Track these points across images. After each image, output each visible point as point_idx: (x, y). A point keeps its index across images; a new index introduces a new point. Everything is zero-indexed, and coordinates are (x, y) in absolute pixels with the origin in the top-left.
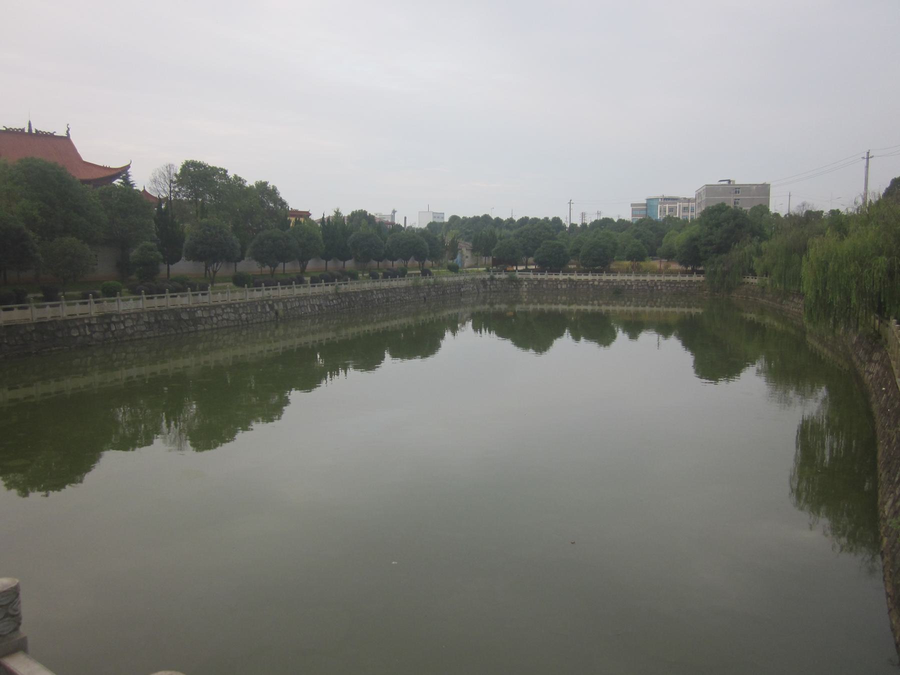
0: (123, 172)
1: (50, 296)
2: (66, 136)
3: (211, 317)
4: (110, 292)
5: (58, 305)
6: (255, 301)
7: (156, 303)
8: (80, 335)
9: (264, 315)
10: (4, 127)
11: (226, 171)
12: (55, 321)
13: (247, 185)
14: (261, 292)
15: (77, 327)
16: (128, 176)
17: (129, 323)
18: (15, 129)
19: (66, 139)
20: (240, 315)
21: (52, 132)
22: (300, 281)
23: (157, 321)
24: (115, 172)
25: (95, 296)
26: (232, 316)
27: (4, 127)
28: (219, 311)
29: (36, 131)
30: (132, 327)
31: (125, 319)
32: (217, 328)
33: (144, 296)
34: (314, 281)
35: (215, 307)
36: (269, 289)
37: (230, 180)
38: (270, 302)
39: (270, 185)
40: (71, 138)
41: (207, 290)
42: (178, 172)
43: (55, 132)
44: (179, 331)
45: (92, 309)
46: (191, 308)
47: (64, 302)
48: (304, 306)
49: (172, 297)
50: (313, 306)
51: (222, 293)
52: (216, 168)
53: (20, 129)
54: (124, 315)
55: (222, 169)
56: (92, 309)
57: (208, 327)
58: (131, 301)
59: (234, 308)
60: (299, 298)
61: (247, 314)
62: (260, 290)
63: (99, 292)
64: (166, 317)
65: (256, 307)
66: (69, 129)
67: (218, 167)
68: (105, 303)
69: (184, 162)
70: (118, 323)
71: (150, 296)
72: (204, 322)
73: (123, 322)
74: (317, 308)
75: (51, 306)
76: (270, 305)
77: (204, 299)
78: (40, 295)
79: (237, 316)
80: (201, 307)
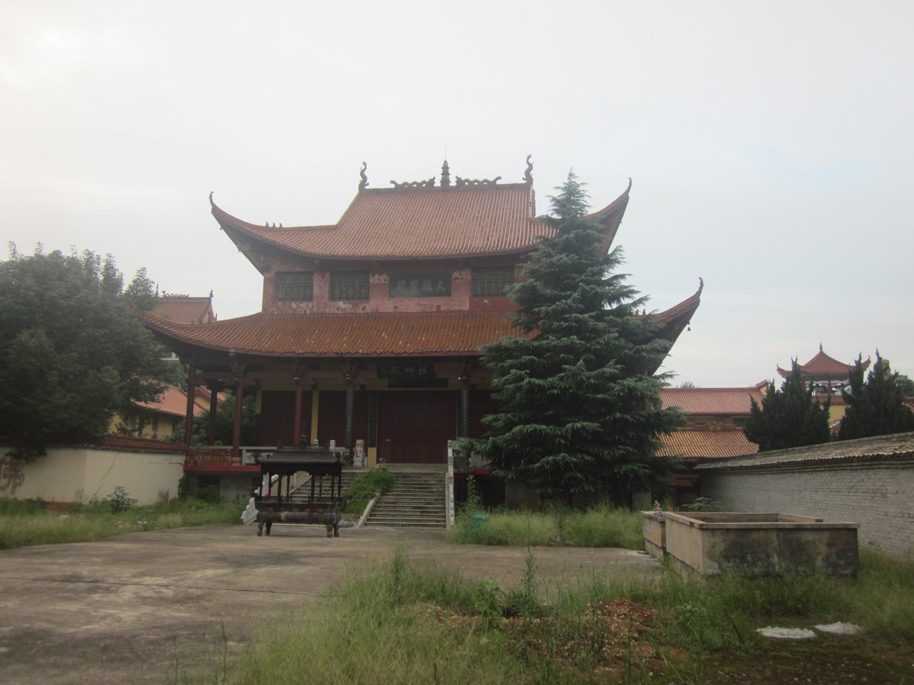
2: (524, 182)
10: (392, 182)
18: (415, 183)
21: (491, 179)
27: (392, 182)
29: (459, 181)
40: (535, 186)
43: (499, 178)
53: (424, 182)
66: (531, 167)
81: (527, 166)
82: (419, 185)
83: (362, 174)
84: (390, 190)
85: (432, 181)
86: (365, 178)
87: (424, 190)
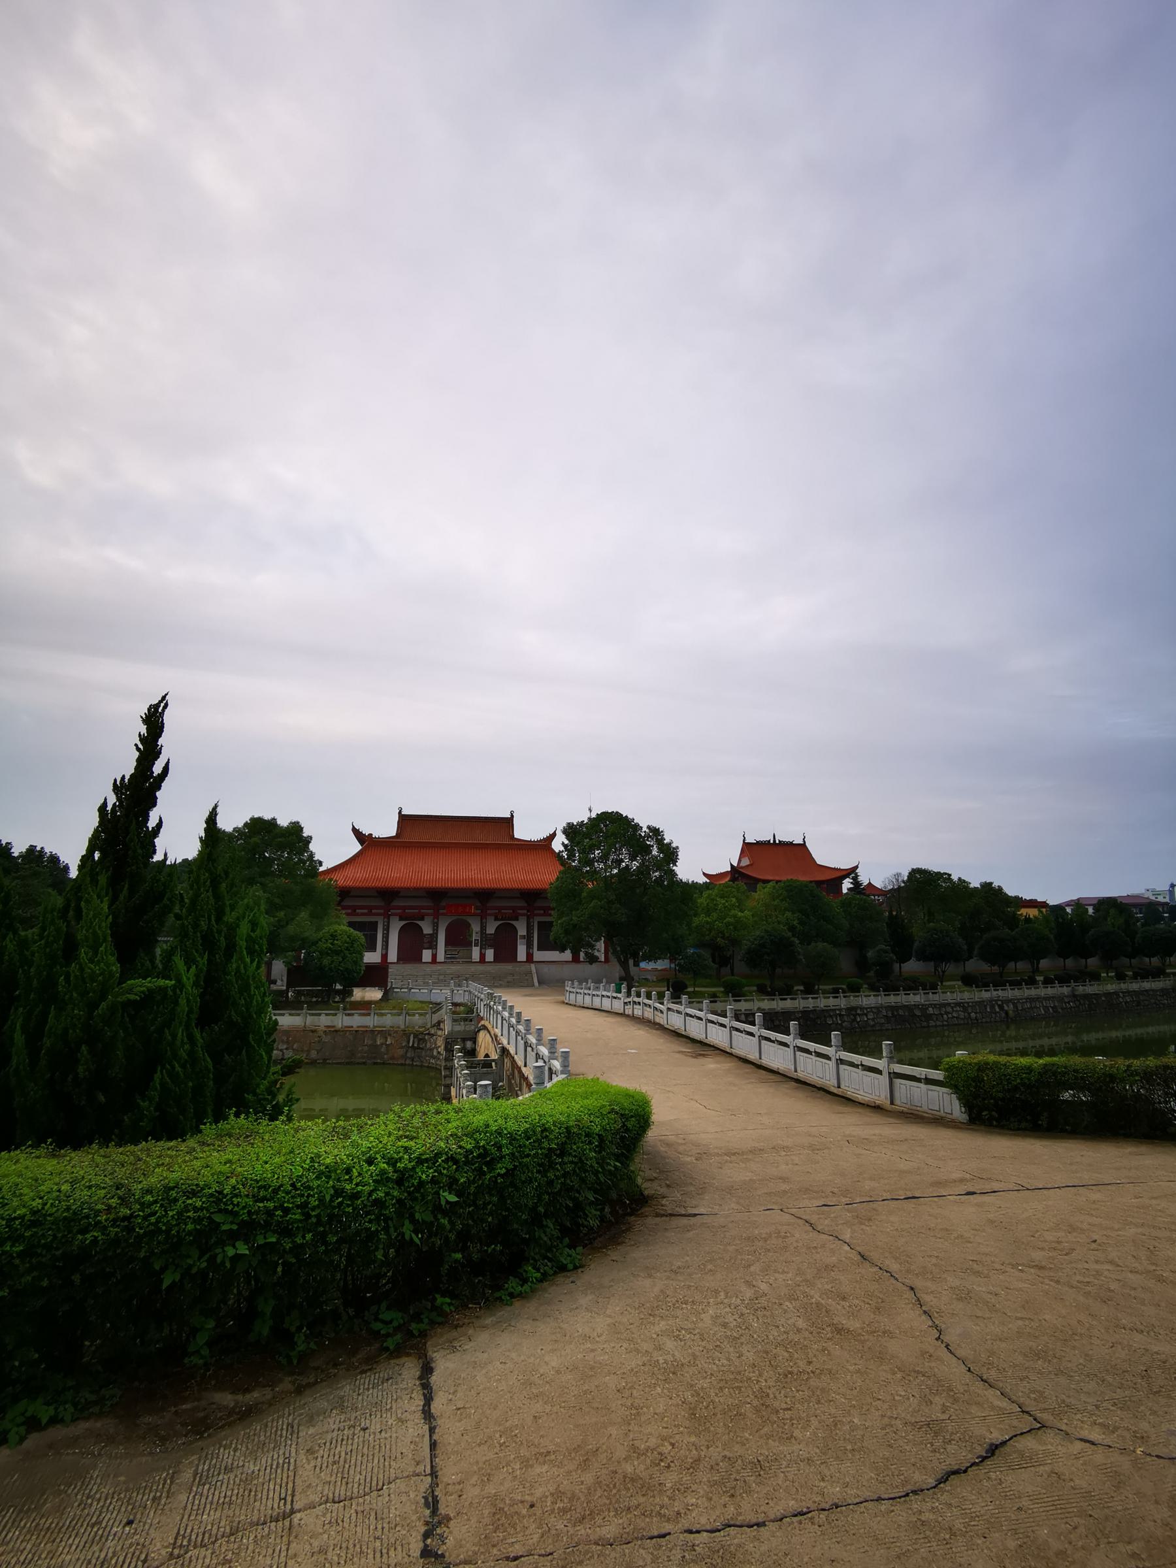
0: (852, 872)
1: (809, 990)
3: (942, 1015)
4: (855, 989)
5: (817, 998)
6: (984, 1001)
7: (892, 999)
8: (833, 1023)
9: (994, 1015)
11: (950, 875)
12: (815, 1010)
13: (972, 886)
14: (989, 993)
15: (831, 1016)
16: (857, 876)
17: (871, 1016)
19: (803, 846)
20: (969, 1014)
22: (1032, 982)
23: (893, 1015)
24: (845, 873)
25: (844, 992)
26: (962, 1015)
28: (949, 1009)
30: (873, 1019)
31: (868, 1012)
32: (948, 1025)
33: (882, 993)
34: (1048, 982)
35: (945, 1005)
36: (998, 990)
37: (954, 883)
38: (1000, 1003)
39: (996, 884)
41: (937, 989)
42: (906, 878)
44: (914, 1026)
46: (923, 1005)
48: (1036, 1007)
49: (905, 994)
50: (1046, 1008)
51: (951, 992)
52: (940, 872)
54: (866, 1009)
55: (946, 874)
57: (938, 1023)
58: (872, 997)
59: (964, 1006)
60: (1031, 999)
61: (976, 1013)
62: (988, 990)
63: (844, 987)
64: (901, 1012)
65: (985, 1006)
67: (942, 872)
68: (852, 998)
69: (910, 870)
70: (862, 1015)
72: (935, 1019)
73: (866, 1015)
74: (1051, 1009)
75: (812, 998)
76: (999, 1006)
77: (934, 998)
78: (802, 988)
79: (966, 1014)
80: (931, 1004)
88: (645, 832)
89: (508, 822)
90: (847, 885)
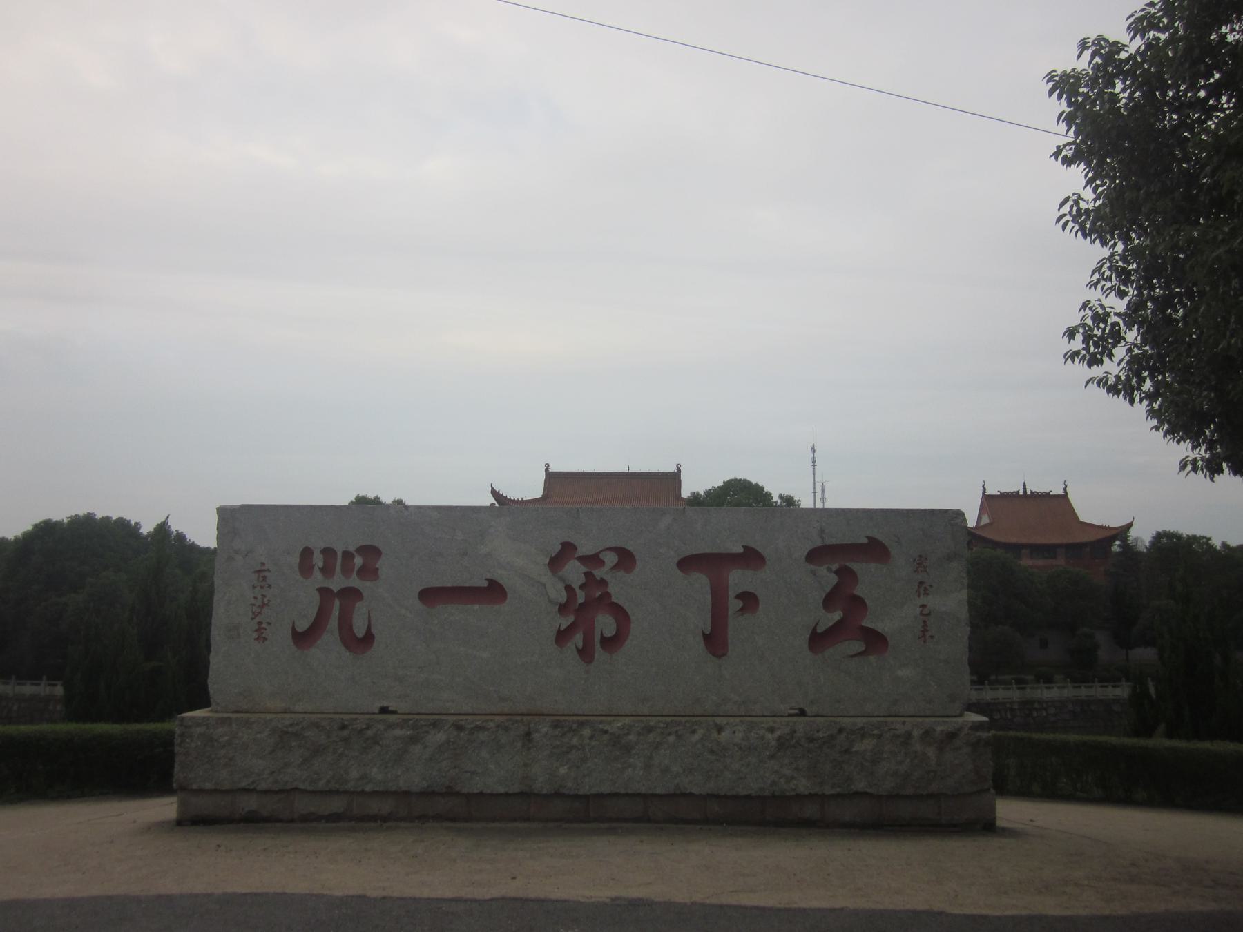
5: (982, 689)
7: (1084, 692)
10: (999, 491)
19: (1064, 497)
24: (1114, 532)
27: (999, 491)
29: (1031, 492)
42: (1147, 544)
45: (1015, 695)
47: (987, 687)
49: (1102, 686)
53: (1014, 492)
55: (1204, 537)
56: (1015, 695)
58: (1055, 689)
66: (1066, 486)
67: (1198, 535)
68: (1028, 690)
71: (1076, 685)
81: (1064, 486)
82: (1012, 493)
83: (983, 487)
84: (998, 495)
85: (1018, 491)
86: (985, 489)
87: (1015, 495)
88: (776, 502)
89: (674, 479)
90: (1116, 547)
